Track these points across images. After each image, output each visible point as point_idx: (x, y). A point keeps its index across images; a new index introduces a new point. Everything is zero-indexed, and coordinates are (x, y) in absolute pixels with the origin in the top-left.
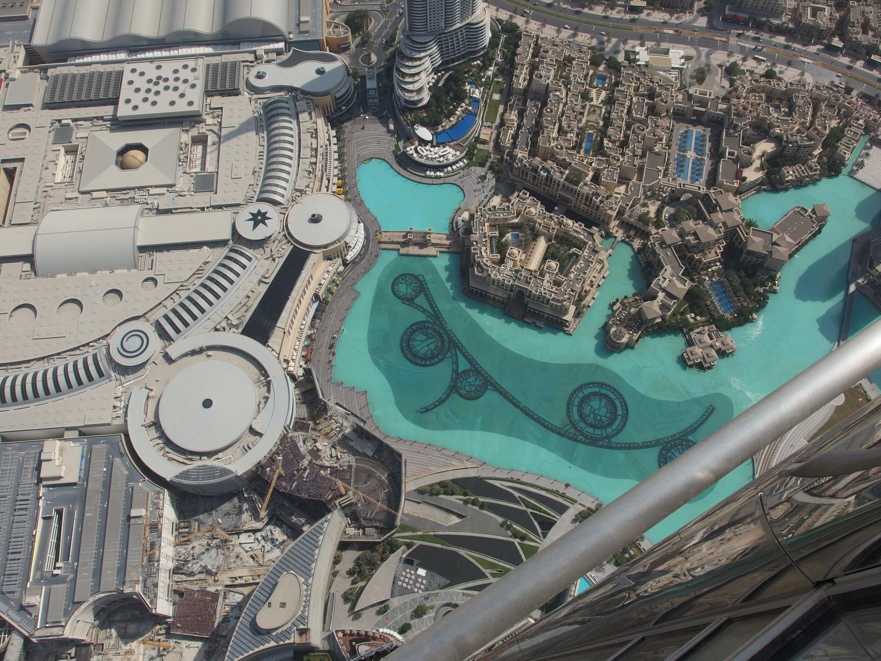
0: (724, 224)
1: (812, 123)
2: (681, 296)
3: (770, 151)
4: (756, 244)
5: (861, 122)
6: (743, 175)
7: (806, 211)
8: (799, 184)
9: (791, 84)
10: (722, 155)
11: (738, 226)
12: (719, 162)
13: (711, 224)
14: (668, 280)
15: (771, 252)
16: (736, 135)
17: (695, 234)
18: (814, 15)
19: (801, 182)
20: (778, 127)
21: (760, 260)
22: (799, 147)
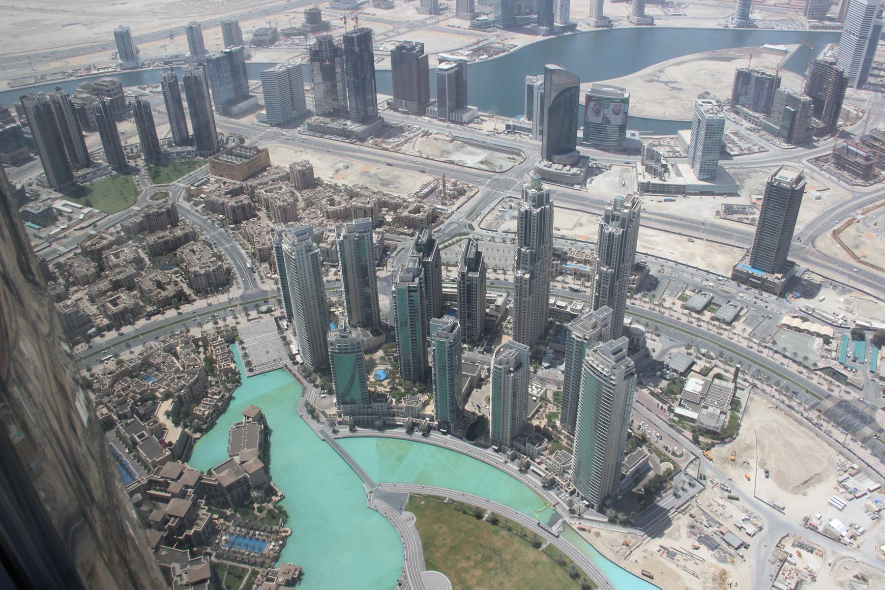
0: (187, 487)
1: (183, 366)
2: (208, 574)
3: (170, 409)
4: (227, 478)
5: (219, 339)
6: (167, 441)
7: (242, 423)
8: (219, 411)
9: (140, 354)
10: (135, 443)
11: (200, 478)
12: (138, 451)
13: (174, 496)
14: (184, 575)
15: (246, 472)
16: (132, 420)
17: (171, 516)
18: (115, 305)
19: (219, 410)
20: (160, 387)
21: (245, 486)
22: (190, 387)
